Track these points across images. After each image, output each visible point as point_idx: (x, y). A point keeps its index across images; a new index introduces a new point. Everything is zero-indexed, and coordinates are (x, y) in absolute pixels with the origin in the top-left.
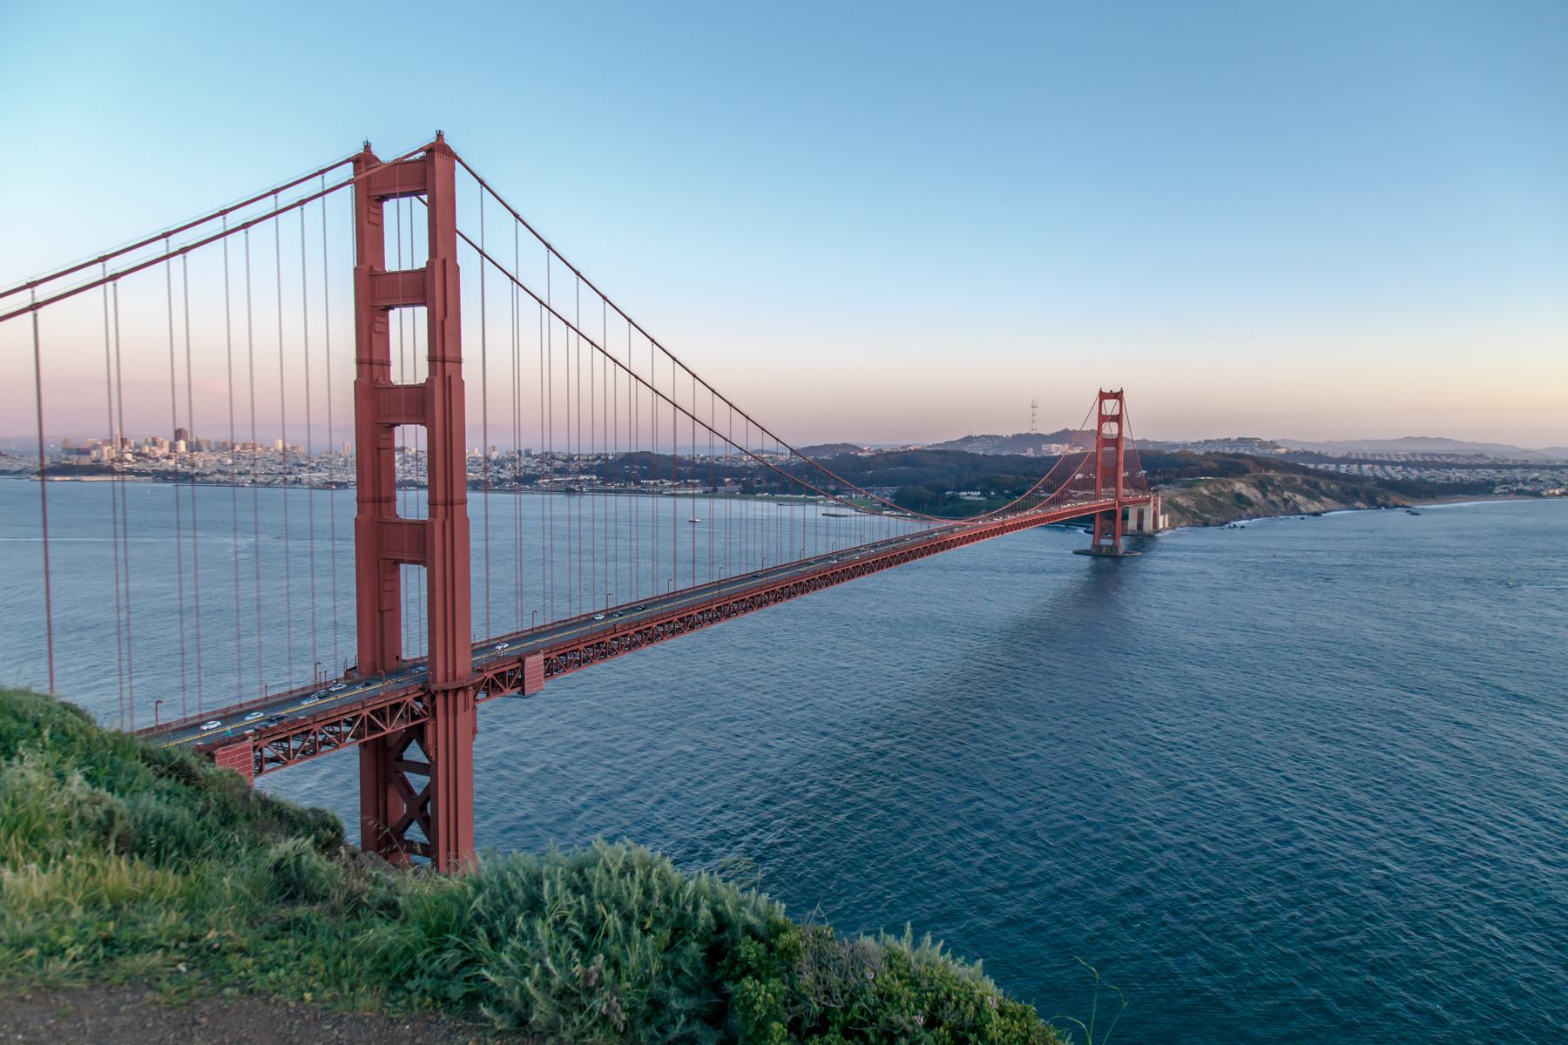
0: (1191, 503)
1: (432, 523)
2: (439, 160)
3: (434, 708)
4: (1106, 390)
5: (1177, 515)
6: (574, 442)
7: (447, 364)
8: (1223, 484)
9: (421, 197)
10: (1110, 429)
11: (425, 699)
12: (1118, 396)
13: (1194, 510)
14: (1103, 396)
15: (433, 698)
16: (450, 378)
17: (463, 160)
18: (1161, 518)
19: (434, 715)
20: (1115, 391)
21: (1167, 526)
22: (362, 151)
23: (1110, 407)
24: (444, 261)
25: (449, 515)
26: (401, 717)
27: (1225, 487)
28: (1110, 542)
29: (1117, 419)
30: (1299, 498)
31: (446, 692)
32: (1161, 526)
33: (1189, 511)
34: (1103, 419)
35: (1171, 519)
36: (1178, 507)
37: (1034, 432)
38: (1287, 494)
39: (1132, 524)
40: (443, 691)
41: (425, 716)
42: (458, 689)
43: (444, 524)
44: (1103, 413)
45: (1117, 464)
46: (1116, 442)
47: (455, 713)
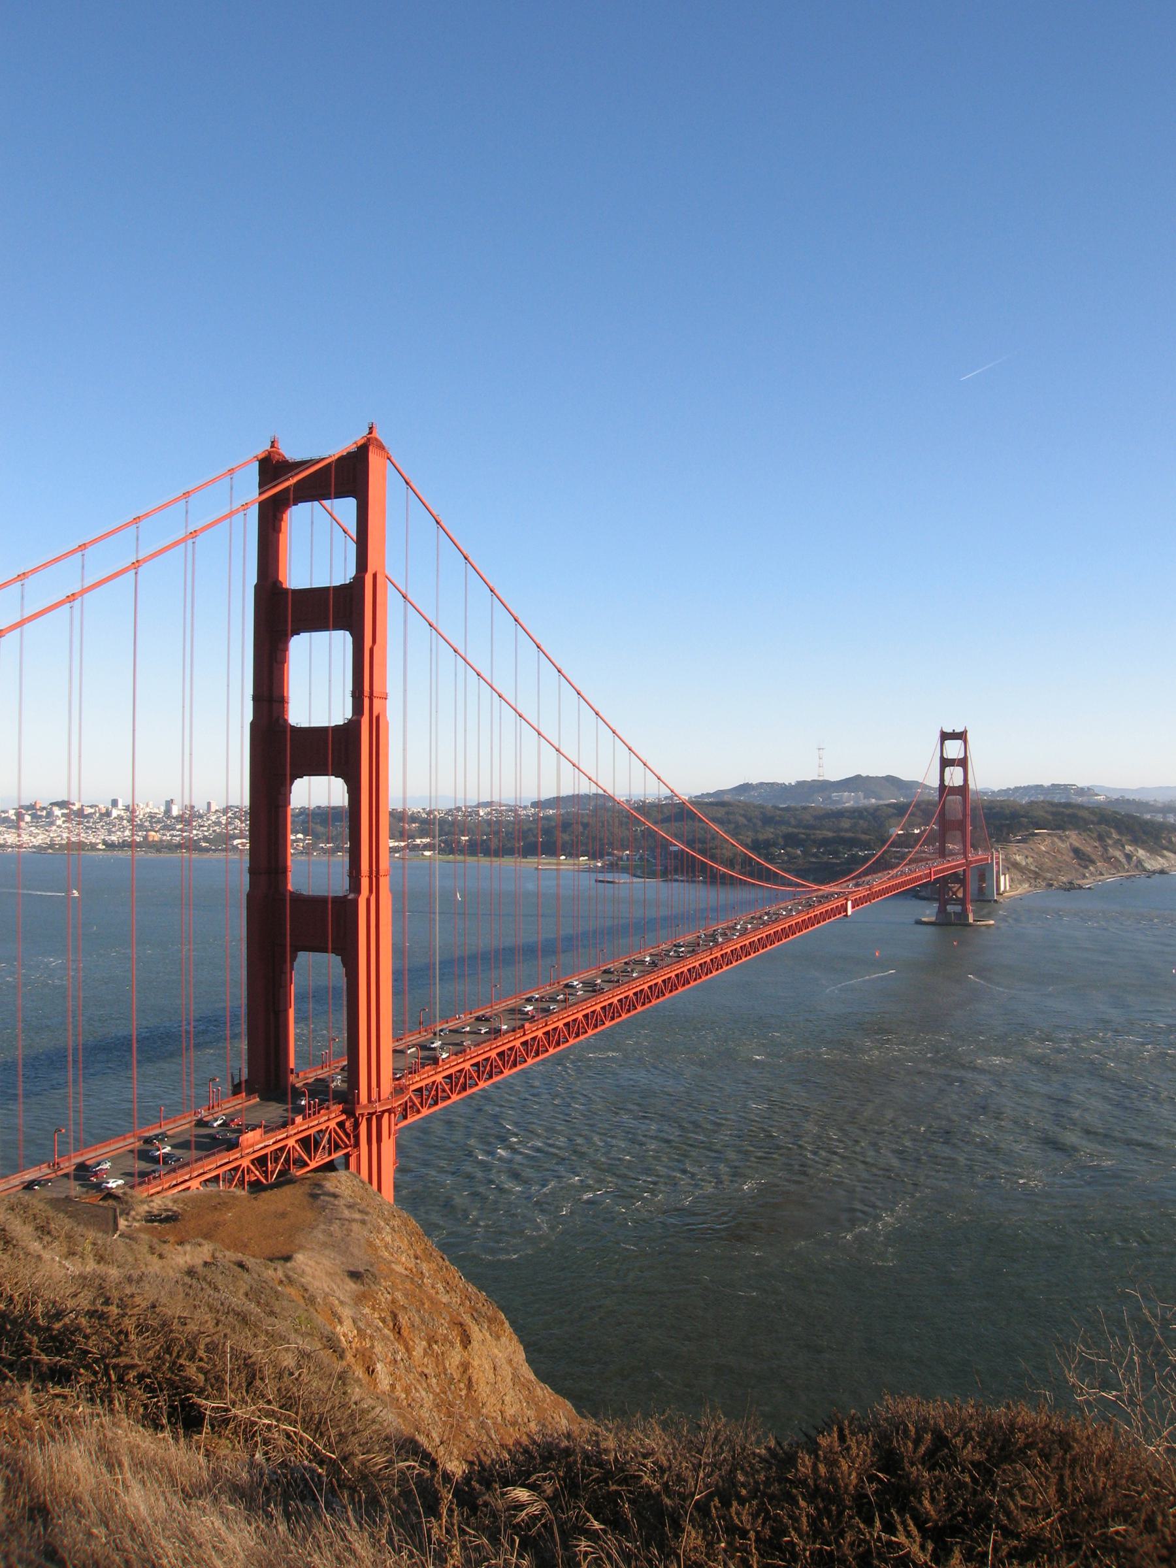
0: (1030, 860)
1: (355, 903)
2: (374, 458)
3: (357, 1137)
4: (951, 731)
5: (1018, 875)
6: (460, 795)
7: (375, 700)
8: (1060, 838)
9: (324, 502)
10: (954, 777)
11: (348, 1124)
12: (961, 736)
13: (1033, 868)
14: (945, 736)
15: (356, 1125)
16: (378, 718)
17: (393, 459)
18: (1002, 878)
19: (357, 1145)
20: (956, 731)
21: (1008, 888)
22: (268, 448)
23: (954, 749)
24: (375, 576)
25: (375, 888)
26: (324, 1148)
27: (1063, 841)
28: (958, 908)
29: (963, 763)
30: (1141, 853)
31: (372, 1114)
32: (1002, 888)
33: (1030, 871)
34: (945, 763)
35: (1012, 880)
36: (1016, 865)
37: (821, 778)
38: (1128, 848)
39: (972, 886)
40: (369, 1114)
41: (347, 1146)
42: (384, 1112)
43: (368, 901)
44: (945, 756)
45: (965, 815)
46: (963, 790)
47: (379, 1140)
